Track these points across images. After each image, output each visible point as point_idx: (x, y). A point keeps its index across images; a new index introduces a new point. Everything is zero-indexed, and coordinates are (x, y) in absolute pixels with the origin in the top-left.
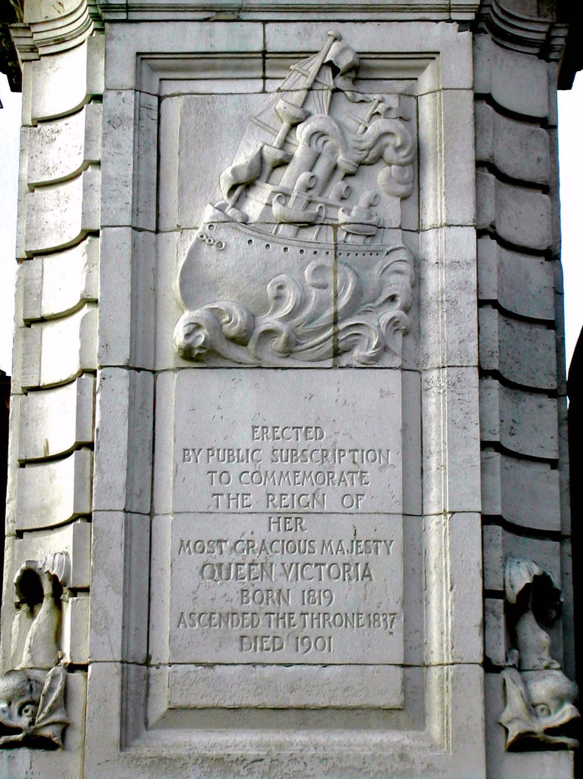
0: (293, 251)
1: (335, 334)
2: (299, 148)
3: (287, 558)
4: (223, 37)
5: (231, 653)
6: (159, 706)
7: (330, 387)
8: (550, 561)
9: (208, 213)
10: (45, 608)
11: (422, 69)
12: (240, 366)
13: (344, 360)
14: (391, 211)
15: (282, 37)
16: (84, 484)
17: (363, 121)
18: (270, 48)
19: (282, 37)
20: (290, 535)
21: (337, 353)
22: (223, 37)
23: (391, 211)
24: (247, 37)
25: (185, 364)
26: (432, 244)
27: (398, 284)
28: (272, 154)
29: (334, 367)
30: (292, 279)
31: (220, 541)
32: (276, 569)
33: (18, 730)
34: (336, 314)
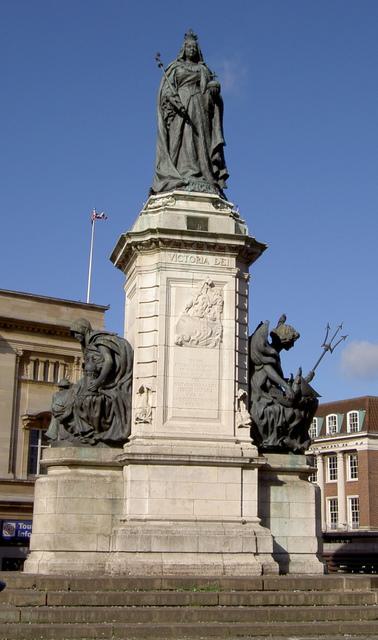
4: (184, 275)
5: (184, 406)
6: (169, 416)
7: (205, 351)
9: (181, 313)
10: (144, 394)
14: (218, 315)
15: (197, 276)
16: (155, 369)
17: (212, 295)
19: (197, 276)
22: (184, 275)
23: (218, 315)
24: (189, 275)
26: (225, 323)
27: (219, 331)
28: (195, 302)
30: (197, 329)
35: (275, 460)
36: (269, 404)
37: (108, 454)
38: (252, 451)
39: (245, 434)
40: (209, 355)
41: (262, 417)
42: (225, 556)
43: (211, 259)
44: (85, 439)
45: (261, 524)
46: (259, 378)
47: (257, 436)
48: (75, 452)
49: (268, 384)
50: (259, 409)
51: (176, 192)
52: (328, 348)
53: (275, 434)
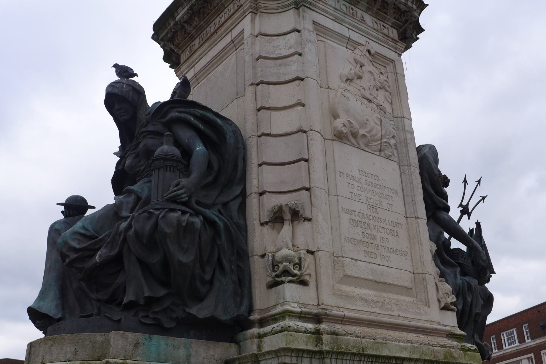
0: (369, 109)
1: (381, 143)
3: (376, 223)
5: (362, 256)
11: (389, 64)
12: (353, 145)
13: (382, 154)
15: (355, 36)
18: (351, 37)
20: (374, 214)
21: (380, 150)
25: (335, 138)
29: (380, 155)
31: (354, 211)
32: (372, 227)
33: (295, 275)
34: (382, 135)
39: (450, 320)
48: (136, 345)
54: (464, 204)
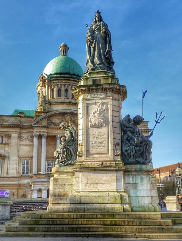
2: (98, 110)
8: (119, 141)
28: (96, 111)
35: (129, 167)
36: (129, 146)
37: (69, 169)
38: (121, 164)
39: (119, 158)
40: (104, 130)
41: (126, 151)
42: (109, 205)
43: (102, 95)
44: (64, 163)
45: (125, 192)
46: (125, 137)
47: (124, 157)
49: (129, 138)
50: (124, 149)
51: (91, 71)
52: (157, 122)
53: (132, 157)
54: (156, 121)
